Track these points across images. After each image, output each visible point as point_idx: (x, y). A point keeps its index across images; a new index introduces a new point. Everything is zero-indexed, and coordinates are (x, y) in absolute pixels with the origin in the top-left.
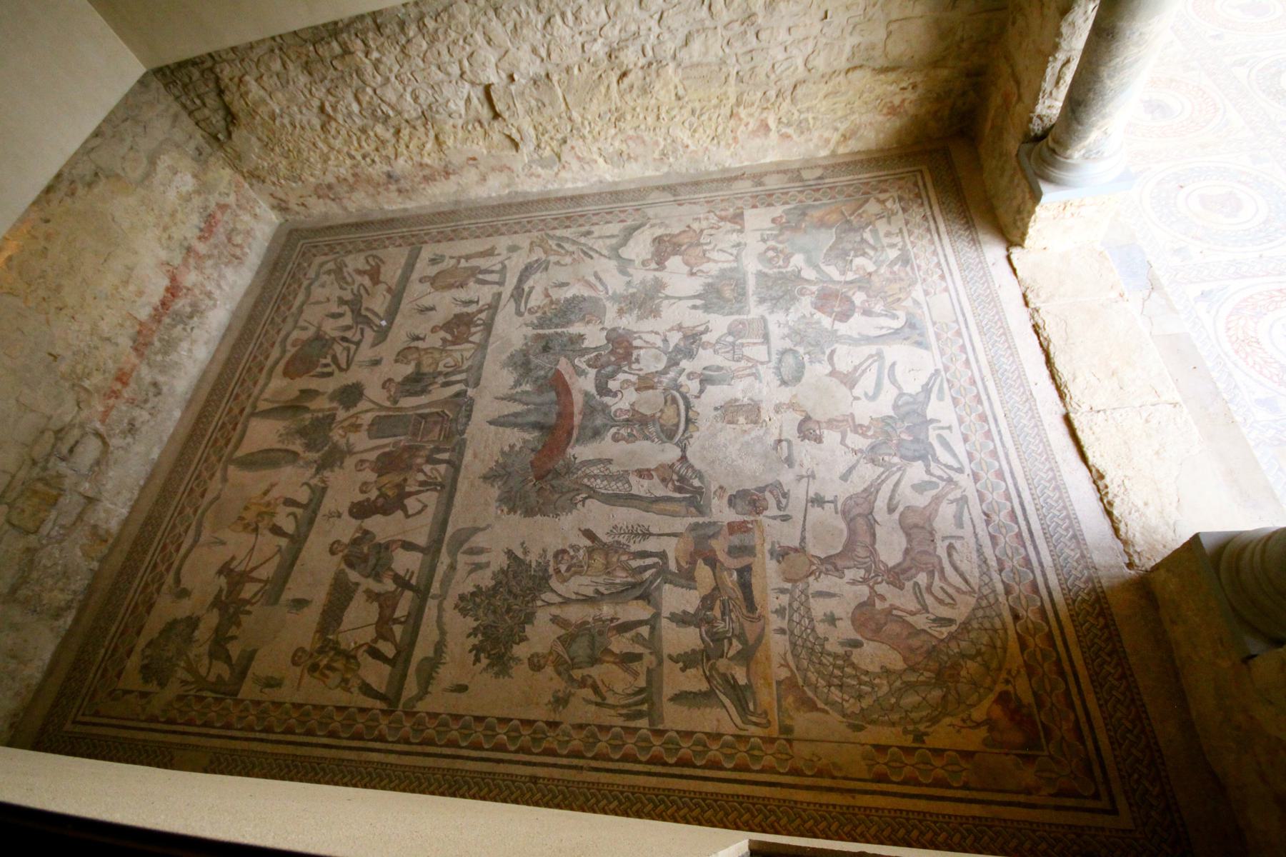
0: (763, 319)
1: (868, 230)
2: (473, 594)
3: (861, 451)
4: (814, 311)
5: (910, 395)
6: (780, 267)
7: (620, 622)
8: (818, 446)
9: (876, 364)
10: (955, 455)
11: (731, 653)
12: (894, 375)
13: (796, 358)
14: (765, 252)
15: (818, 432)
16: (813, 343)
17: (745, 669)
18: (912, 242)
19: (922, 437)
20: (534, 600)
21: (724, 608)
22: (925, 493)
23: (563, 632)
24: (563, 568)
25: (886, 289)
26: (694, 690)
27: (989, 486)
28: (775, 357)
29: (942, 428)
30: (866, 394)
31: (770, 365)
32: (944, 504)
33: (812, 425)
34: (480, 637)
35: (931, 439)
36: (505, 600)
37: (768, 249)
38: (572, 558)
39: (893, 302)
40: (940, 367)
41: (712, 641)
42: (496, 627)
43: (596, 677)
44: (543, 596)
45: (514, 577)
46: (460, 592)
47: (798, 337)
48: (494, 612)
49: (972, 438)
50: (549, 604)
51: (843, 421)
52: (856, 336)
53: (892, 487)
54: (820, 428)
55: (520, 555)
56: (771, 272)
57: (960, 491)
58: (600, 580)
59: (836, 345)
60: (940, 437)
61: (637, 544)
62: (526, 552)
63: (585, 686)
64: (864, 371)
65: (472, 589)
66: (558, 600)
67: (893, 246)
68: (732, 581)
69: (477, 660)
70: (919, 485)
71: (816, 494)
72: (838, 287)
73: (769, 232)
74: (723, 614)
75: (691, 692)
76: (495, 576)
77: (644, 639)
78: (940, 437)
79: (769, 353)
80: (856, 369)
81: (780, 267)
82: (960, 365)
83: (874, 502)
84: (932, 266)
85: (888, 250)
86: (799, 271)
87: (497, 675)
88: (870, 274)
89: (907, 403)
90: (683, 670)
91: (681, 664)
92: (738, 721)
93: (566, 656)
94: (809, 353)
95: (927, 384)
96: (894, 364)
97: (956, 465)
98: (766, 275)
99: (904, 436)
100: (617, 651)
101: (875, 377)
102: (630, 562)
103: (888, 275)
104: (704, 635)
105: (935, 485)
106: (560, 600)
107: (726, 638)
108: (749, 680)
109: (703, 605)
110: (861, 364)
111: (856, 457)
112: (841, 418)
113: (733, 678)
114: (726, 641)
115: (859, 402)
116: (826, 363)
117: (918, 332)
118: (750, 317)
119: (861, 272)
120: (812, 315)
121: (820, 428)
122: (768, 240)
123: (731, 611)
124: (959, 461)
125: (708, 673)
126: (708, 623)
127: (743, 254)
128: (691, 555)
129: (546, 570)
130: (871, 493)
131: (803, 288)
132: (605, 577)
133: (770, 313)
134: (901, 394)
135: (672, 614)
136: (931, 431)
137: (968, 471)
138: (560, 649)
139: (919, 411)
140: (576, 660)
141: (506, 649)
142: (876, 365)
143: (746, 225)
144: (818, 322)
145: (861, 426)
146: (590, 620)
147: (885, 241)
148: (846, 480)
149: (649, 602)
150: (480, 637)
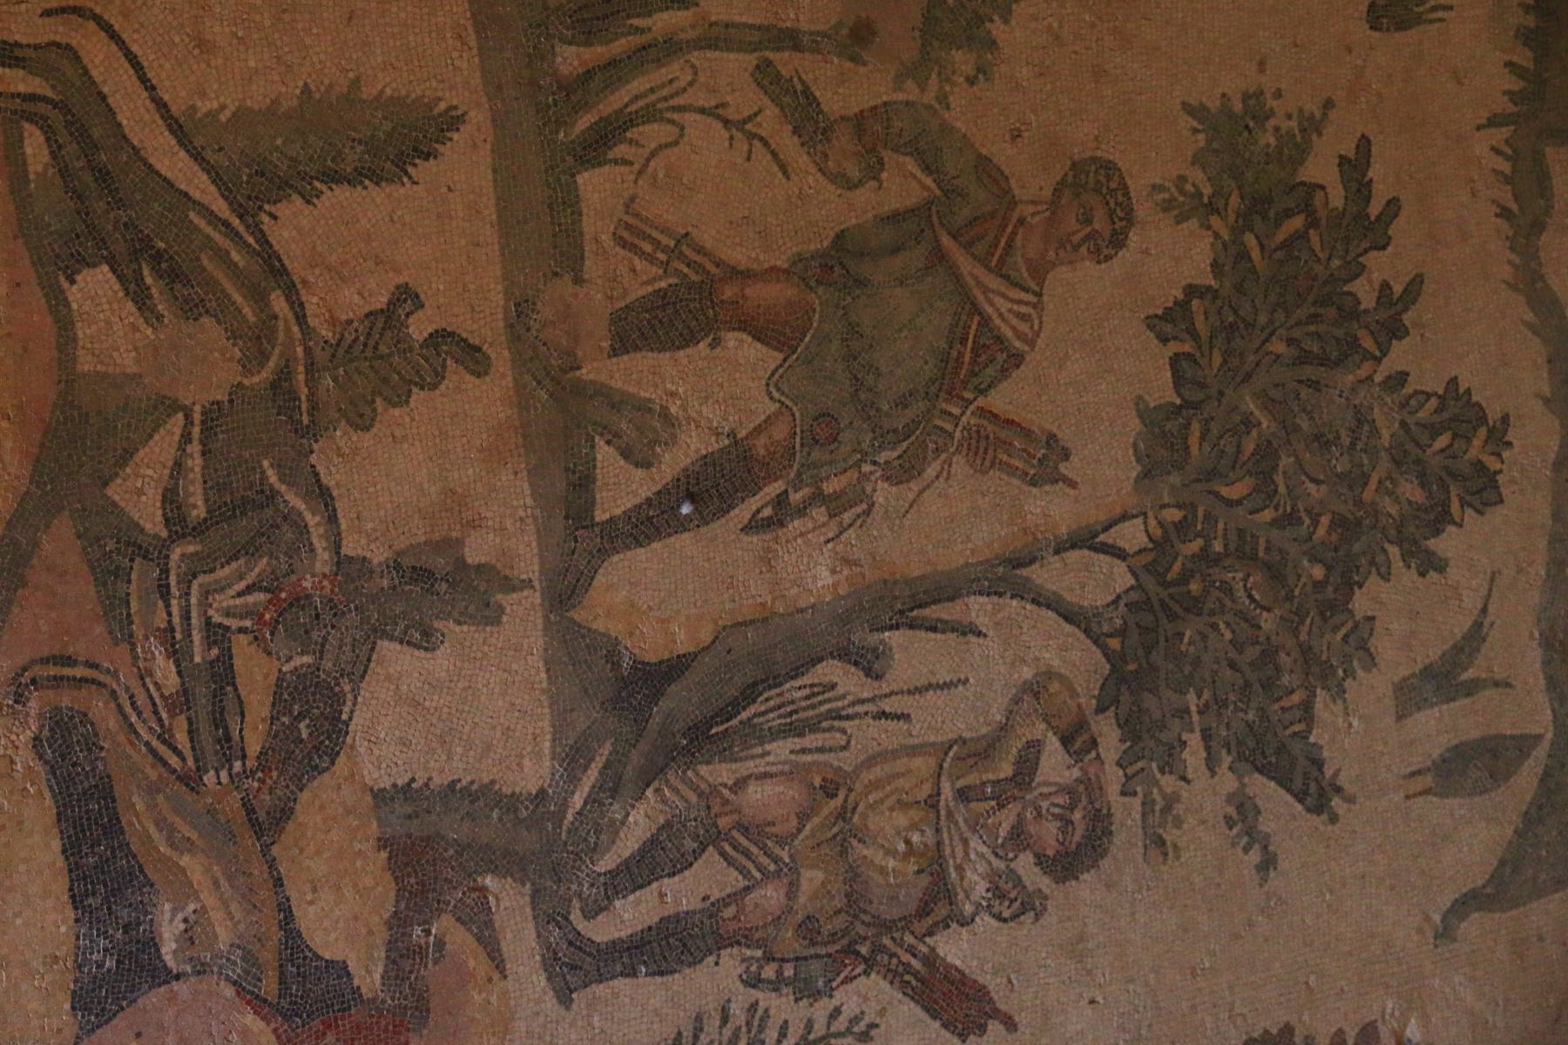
2: (1440, 519)
7: (742, 513)
11: (161, 447)
17: (85, 364)
20: (1161, 546)
21: (219, 721)
23: (998, 400)
24: (1055, 766)
26: (342, 193)
34: (1364, 291)
36: (1291, 519)
38: (1019, 839)
41: (274, 494)
42: (1304, 359)
43: (814, 179)
44: (1122, 578)
45: (1269, 654)
46: (1496, 515)
48: (1321, 441)
50: (1086, 539)
55: (1264, 789)
58: (869, 735)
61: (712, 1005)
62: (1243, 812)
63: (858, 122)
65: (1446, 544)
66: (1048, 575)
68: (191, 892)
69: (1355, 167)
74: (222, 673)
75: (355, 178)
76: (1360, 644)
77: (613, 438)
87: (1256, 109)
90: (406, 298)
91: (419, 328)
92: (97, 53)
93: (966, 265)
100: (739, 346)
102: (735, 880)
104: (311, 520)
106: (1035, 574)
107: (199, 530)
108: (57, 302)
109: (337, 699)
113: (142, 299)
114: (199, 512)
123: (182, 701)
125: (279, 304)
126: (300, 600)
128: (422, 1008)
129: (1131, 729)
132: (846, 761)
135: (491, 616)
138: (1001, 305)
140: (916, 256)
141: (1244, 255)
146: (883, 494)
149: (612, 655)
150: (1364, 291)
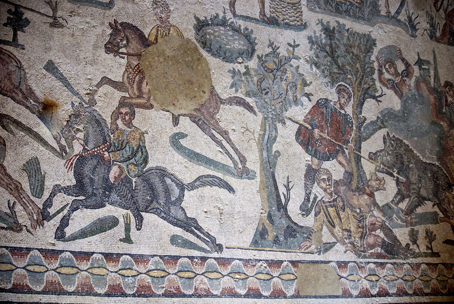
0: (304, 26)
1: (436, 209)
3: (92, 103)
4: (315, 99)
5: (180, 199)
6: (381, 73)
8: (102, 45)
9: (230, 163)
10: (83, 234)
12: (212, 185)
13: (241, 54)
14: (403, 60)
15: (123, 50)
16: (264, 85)
18: (418, 265)
19: (114, 197)
22: (25, 174)
25: (348, 210)
27: (37, 268)
28: (242, 24)
29: (128, 229)
30: (183, 136)
31: (229, 15)
32: (7, 196)
33: (135, 46)
35: (108, 207)
37: (407, 65)
39: (328, 215)
40: (226, 254)
47: (271, 66)
49: (111, 267)
51: (139, 89)
52: (275, 147)
53: (35, 130)
54: (129, 54)
56: (373, 58)
57: (29, 224)
59: (260, 116)
60: (114, 222)
64: (219, 143)
67: (414, 236)
70: (39, 169)
71: (27, 22)
72: (351, 145)
73: (432, 72)
78: (114, 222)
79: (246, 18)
80: (225, 134)
81: (381, 73)
82: (227, 282)
83: (13, 98)
84: (383, 283)
85: (407, 230)
86: (374, 97)
88: (371, 195)
89: (167, 191)
94: (247, 73)
95: (199, 229)
96: (230, 189)
97: (69, 231)
98: (369, 50)
99: (114, 171)
101: (210, 156)
103: (368, 221)
105: (39, 193)
110: (229, 141)
111: (83, 92)
112: (145, 88)
115: (170, 123)
116: (232, 93)
117: (282, 239)
118: (304, 9)
119: (374, 183)
120: (308, 95)
121: (129, 54)
122: (420, 68)
124: (74, 238)
127: (399, 29)
130: (26, 98)
131: (350, 97)
133: (310, 38)
134: (182, 187)
136: (125, 211)
137: (60, 246)
139: (155, 205)
142: (230, 163)
143: (441, 46)
144: (296, 102)
145: (133, 114)
147: (421, 229)
148: (47, 70)
